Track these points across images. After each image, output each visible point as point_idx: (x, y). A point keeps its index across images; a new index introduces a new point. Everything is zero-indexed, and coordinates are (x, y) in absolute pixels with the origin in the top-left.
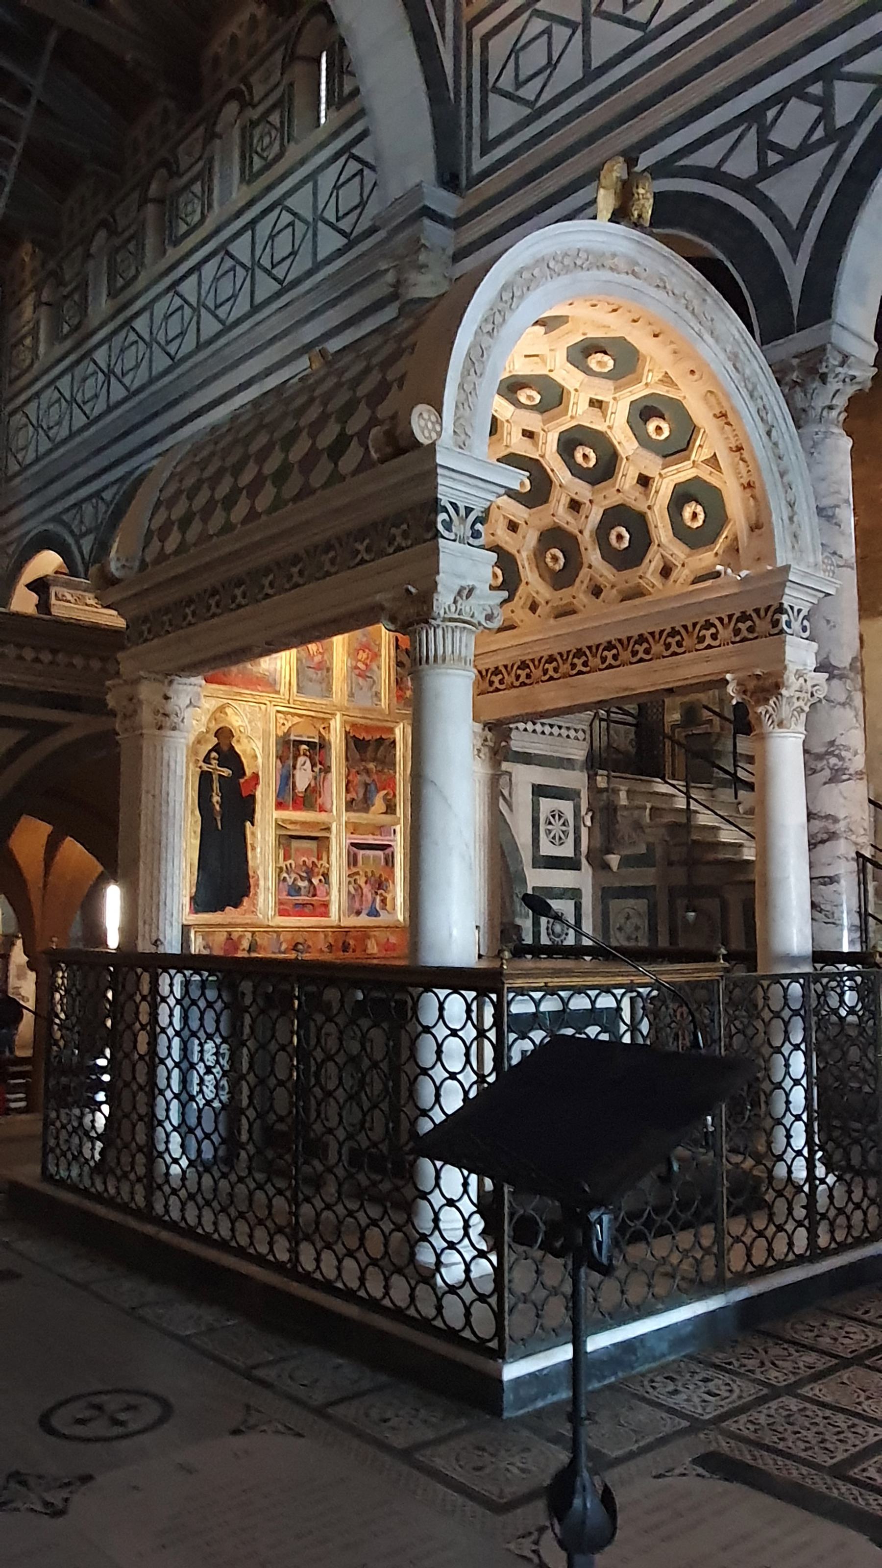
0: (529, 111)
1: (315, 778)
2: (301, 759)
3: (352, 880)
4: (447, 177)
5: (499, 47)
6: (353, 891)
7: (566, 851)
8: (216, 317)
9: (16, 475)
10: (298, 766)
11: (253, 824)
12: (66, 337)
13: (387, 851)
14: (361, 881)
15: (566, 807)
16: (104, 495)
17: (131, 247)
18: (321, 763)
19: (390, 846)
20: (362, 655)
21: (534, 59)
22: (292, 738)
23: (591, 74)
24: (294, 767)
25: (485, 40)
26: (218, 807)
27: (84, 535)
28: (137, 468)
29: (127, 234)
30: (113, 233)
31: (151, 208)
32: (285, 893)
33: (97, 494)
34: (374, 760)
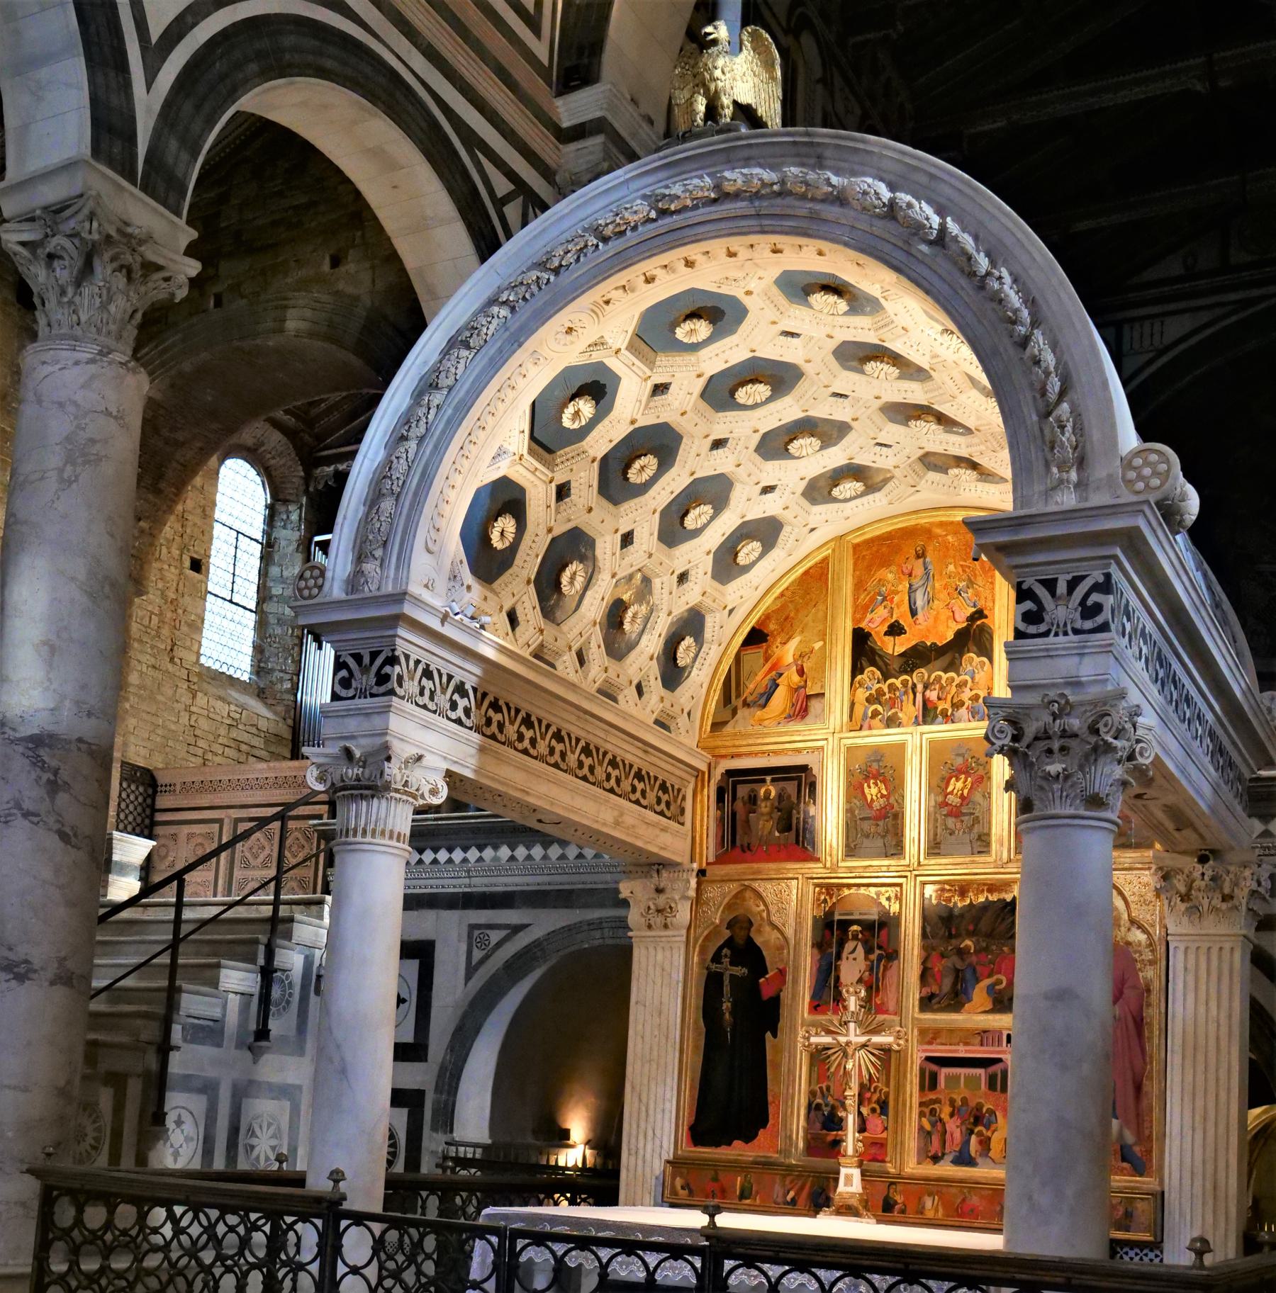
1: (871, 970)
2: (849, 946)
3: (927, 1110)
6: (928, 1127)
10: (844, 955)
11: (775, 1035)
13: (992, 1069)
14: (945, 1112)
18: (880, 947)
19: (1000, 1060)
20: (956, 785)
22: (837, 917)
24: (839, 957)
26: (727, 1016)
32: (818, 1125)
34: (971, 934)
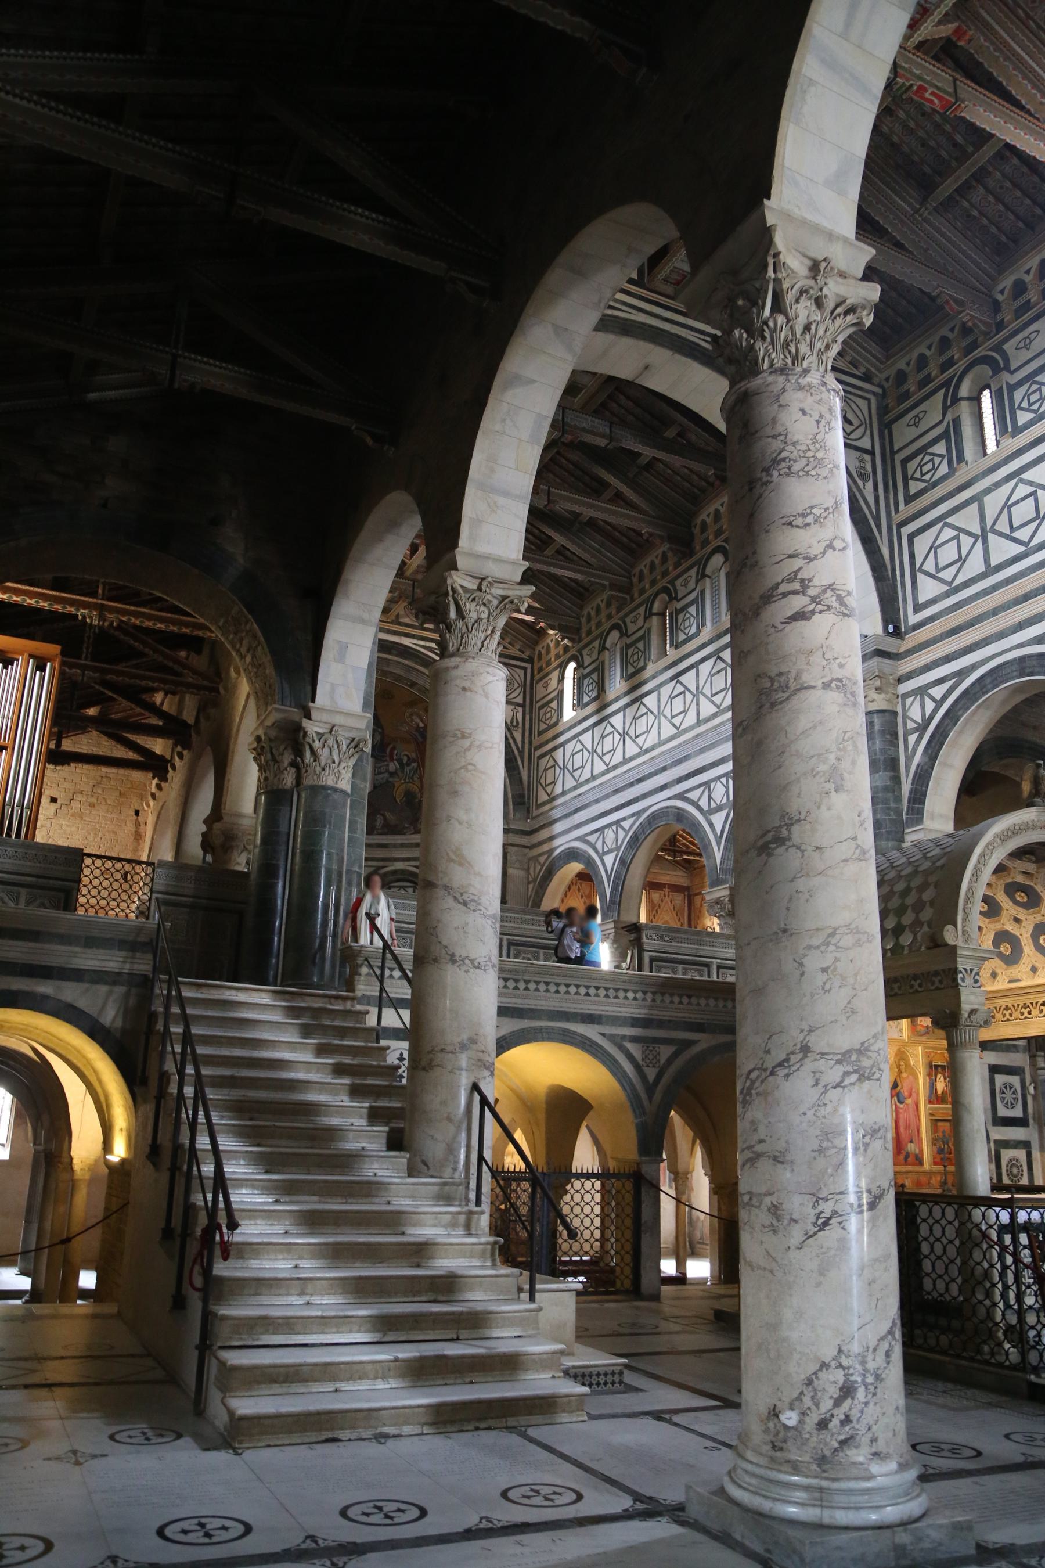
0: (948, 588)
4: (891, 629)
5: (922, 544)
7: (1017, 1112)
8: (713, 702)
9: (545, 803)
12: (587, 704)
15: (1015, 1080)
16: (623, 824)
17: (640, 645)
21: (949, 554)
23: (990, 570)
25: (911, 537)
27: (605, 853)
28: (651, 806)
29: (634, 637)
30: (624, 634)
31: (655, 620)
33: (617, 823)
